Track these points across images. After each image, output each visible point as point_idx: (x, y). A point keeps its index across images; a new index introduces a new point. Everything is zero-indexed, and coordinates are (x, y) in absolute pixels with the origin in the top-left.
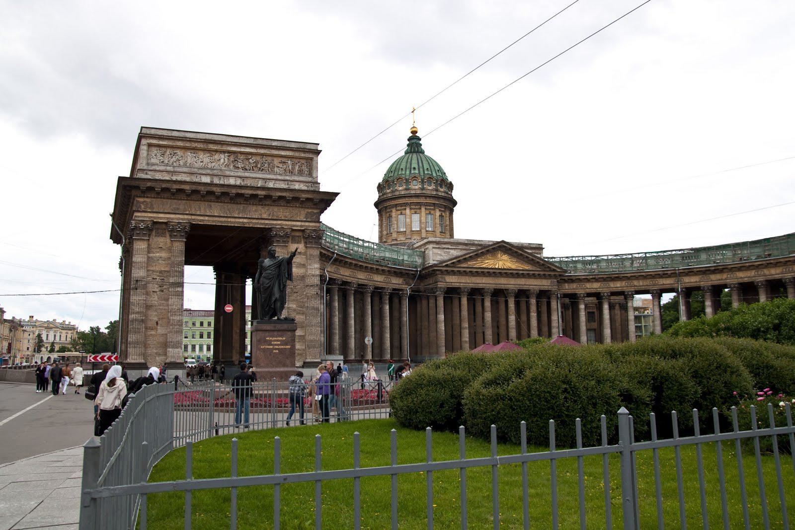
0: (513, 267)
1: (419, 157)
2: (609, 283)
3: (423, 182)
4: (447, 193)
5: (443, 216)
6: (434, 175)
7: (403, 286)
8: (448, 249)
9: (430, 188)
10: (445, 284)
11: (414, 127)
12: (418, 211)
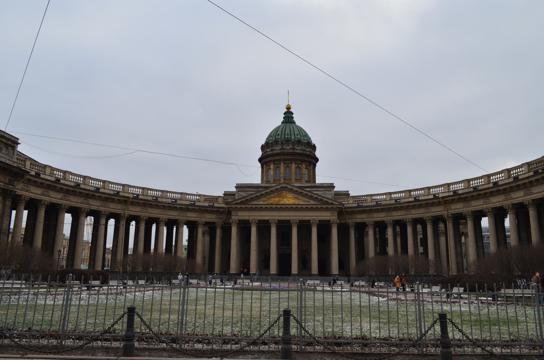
0: (297, 203)
1: (285, 126)
2: (392, 212)
3: (282, 144)
4: (304, 150)
5: (300, 167)
6: (293, 137)
7: (217, 220)
8: (251, 191)
9: (288, 148)
10: (237, 217)
11: (289, 105)
12: (279, 165)
